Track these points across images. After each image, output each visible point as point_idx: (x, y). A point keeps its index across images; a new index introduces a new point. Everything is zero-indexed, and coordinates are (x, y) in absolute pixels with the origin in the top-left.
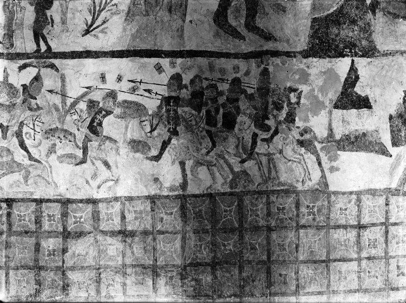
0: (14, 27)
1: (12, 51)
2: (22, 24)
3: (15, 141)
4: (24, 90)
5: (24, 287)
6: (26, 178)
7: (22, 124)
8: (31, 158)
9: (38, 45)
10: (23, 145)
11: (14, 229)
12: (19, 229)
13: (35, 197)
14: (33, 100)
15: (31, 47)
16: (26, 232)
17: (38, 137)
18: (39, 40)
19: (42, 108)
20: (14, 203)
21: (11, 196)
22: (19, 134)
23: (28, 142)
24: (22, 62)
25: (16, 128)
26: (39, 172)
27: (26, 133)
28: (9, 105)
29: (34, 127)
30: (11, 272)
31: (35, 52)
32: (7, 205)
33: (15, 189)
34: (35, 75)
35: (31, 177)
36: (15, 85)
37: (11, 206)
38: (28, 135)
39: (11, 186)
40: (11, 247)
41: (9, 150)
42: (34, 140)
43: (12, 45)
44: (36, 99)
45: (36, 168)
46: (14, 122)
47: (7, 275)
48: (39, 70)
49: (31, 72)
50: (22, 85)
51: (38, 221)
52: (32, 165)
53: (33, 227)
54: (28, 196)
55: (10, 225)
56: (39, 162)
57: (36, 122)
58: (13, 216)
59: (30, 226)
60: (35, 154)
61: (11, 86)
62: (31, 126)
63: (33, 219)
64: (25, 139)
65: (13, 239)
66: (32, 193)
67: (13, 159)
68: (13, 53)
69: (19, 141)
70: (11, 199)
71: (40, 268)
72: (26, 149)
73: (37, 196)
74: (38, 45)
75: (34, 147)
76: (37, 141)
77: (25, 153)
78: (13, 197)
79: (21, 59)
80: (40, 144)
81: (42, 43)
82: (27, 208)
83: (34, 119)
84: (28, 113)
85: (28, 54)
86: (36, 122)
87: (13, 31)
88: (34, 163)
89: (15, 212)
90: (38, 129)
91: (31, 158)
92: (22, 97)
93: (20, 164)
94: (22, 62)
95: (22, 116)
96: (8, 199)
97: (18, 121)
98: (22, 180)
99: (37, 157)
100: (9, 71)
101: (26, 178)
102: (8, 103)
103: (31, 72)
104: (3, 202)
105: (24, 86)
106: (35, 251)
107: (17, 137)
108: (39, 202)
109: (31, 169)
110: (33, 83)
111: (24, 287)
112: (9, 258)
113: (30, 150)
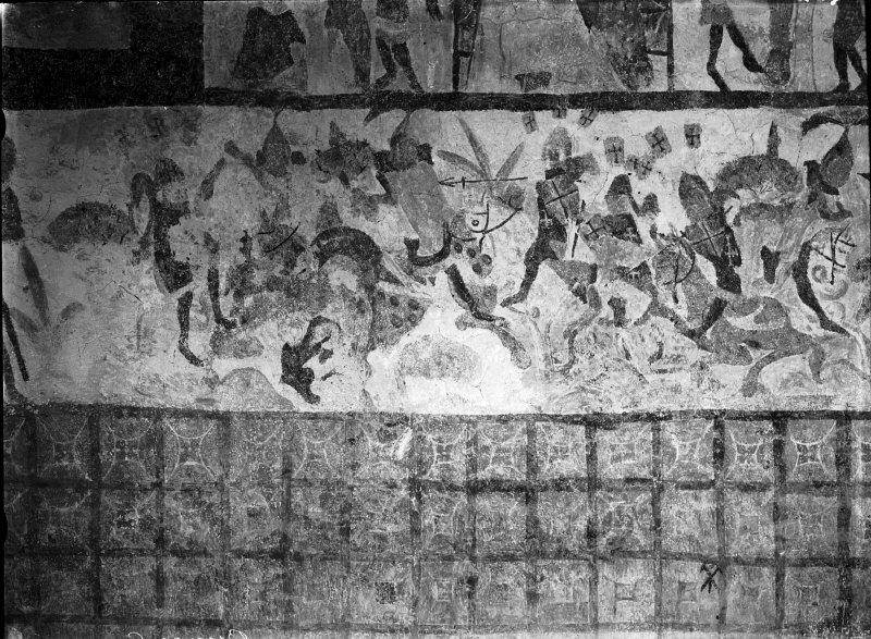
0: (792, 37)
1: (786, 88)
2: (810, 30)
3: (791, 285)
4: (809, 173)
5: (815, 604)
6: (817, 367)
7: (806, 249)
8: (825, 323)
9: (843, 75)
10: (807, 295)
11: (791, 477)
12: (801, 478)
13: (835, 408)
14: (830, 196)
15: (827, 79)
16: (818, 485)
17: (841, 276)
18: (845, 65)
19: (850, 214)
20: (790, 422)
21: (783, 406)
22: (799, 271)
23: (818, 288)
24: (809, 113)
25: (793, 258)
26: (844, 354)
27: (816, 269)
28: (780, 207)
29: (834, 254)
30: (789, 574)
31: (836, 91)
32: (774, 425)
33: (792, 392)
34: (835, 140)
35: (828, 365)
36: (793, 162)
37: (784, 426)
38: (818, 273)
39: (785, 384)
40: (786, 517)
41: (779, 305)
42: (832, 283)
43: (786, 76)
44: (837, 193)
45: (836, 345)
46: (791, 243)
47: (779, 577)
48: (847, 130)
49: (831, 134)
50: (806, 163)
51: (843, 461)
52: (827, 338)
53: (831, 473)
54: (820, 406)
55: (782, 469)
56: (842, 331)
57: (839, 245)
58: (787, 449)
59: (826, 472)
60: (832, 313)
61: (784, 165)
62: (828, 253)
63: (832, 455)
64: (812, 281)
65: (791, 499)
66: (828, 400)
67: (788, 324)
68: (789, 94)
69: (799, 287)
70: (783, 412)
71: (851, 563)
72: (812, 302)
73: (838, 406)
74: (843, 75)
75: (830, 297)
76: (836, 287)
77: (813, 313)
78: (787, 409)
79: (807, 107)
80: (842, 293)
81: (851, 71)
82: (819, 433)
83: (835, 236)
84: (822, 224)
85: (821, 94)
86: (839, 245)
87: (791, 46)
88: (832, 333)
89: (793, 441)
90: (841, 259)
91: (825, 323)
92: (806, 190)
93: (803, 335)
94: (809, 113)
95: (808, 231)
96: (776, 412)
97: (799, 241)
98: (809, 371)
99: (836, 320)
100: (780, 131)
101: (817, 367)
102: (776, 203)
103: (831, 134)
104: (767, 418)
105: (811, 165)
106: (839, 526)
107: (795, 277)
108: (845, 418)
109: (826, 347)
110: (831, 159)
111: (815, 604)
112: (784, 540)
113: (823, 304)
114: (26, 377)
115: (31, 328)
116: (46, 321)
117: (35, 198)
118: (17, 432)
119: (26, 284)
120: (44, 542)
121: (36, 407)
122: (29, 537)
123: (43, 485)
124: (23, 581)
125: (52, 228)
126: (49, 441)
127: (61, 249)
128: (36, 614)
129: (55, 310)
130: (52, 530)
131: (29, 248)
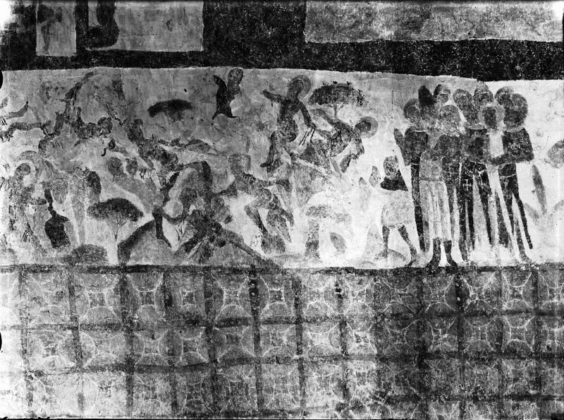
114: (531, 247)
115: (536, 216)
116: (544, 211)
117: (538, 135)
118: (526, 281)
119: (534, 188)
120: (544, 350)
121: (537, 266)
122: (535, 347)
123: (541, 314)
124: (531, 374)
125: (551, 154)
126: (545, 287)
127: (556, 166)
128: (538, 395)
129: (550, 206)
130: (549, 342)
131: (538, 166)
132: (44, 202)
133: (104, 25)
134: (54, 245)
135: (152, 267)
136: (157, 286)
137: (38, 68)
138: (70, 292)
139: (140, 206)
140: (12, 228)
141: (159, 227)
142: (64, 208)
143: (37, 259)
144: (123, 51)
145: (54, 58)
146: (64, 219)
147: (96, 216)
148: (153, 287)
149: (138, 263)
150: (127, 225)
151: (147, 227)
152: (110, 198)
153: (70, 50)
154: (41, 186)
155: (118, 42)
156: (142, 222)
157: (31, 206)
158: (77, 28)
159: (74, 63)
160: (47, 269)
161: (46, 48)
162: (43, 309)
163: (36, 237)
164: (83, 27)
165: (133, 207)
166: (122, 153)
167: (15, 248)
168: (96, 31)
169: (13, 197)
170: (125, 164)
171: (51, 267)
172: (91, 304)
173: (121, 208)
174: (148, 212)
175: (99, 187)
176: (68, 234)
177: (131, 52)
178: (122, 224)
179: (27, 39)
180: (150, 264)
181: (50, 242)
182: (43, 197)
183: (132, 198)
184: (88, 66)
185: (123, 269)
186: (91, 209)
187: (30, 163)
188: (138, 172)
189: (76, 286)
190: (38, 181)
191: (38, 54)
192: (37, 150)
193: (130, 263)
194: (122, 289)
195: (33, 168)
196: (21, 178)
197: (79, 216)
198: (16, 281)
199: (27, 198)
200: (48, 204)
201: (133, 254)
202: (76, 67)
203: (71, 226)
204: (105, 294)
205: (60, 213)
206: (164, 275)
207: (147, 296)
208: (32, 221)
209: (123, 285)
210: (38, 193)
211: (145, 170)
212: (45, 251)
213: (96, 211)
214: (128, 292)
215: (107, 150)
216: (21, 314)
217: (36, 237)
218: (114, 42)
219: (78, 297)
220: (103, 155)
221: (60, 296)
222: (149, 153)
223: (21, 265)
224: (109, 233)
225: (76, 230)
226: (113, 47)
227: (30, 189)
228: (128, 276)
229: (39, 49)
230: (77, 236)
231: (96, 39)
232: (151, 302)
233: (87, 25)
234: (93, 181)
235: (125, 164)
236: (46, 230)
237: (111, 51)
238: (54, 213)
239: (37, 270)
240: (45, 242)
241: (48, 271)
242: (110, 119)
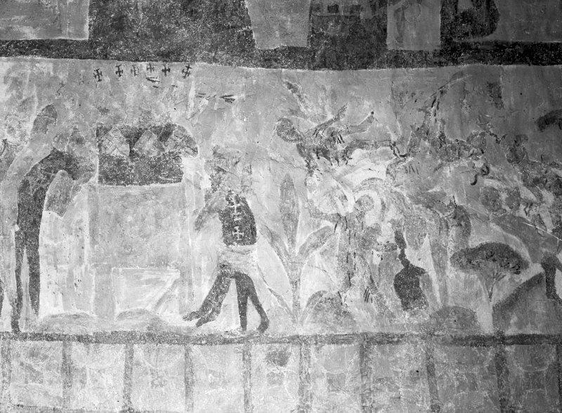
132: (394, 248)
133: (479, 6)
134: (406, 306)
135: (540, 337)
136: (548, 362)
137: (389, 66)
138: (429, 372)
139: (525, 253)
140: (349, 284)
141: (550, 283)
142: (420, 257)
143: (383, 326)
144: (503, 43)
145: (410, 53)
146: (420, 271)
147: (462, 267)
148: (542, 365)
149: (520, 332)
150: (507, 278)
151: (535, 281)
152: (484, 242)
153: (433, 42)
154: (390, 225)
155: (498, 31)
156: (524, 277)
157: (376, 253)
158: (442, 11)
159: (437, 60)
160: (396, 339)
161: (400, 39)
162: (394, 394)
163: (381, 296)
164: (450, 10)
165: (515, 255)
166: (499, 180)
167: (353, 309)
168: (466, 17)
169: (352, 240)
170: (504, 196)
171: (402, 336)
172: (458, 387)
173: (500, 256)
174: (534, 262)
175: (468, 226)
176: (425, 292)
177: (515, 44)
178: (498, 278)
179: (375, 27)
180: (538, 332)
181: (399, 303)
182: (393, 241)
183: (515, 243)
184: (455, 62)
185: (501, 340)
186: (456, 259)
187: (373, 194)
188: (522, 207)
189: (437, 362)
190: (386, 219)
191: (390, 48)
192: (384, 177)
193: (510, 332)
194: (499, 368)
195: (378, 203)
196: (362, 215)
197: (440, 267)
198: (356, 356)
199: (370, 243)
200: (399, 251)
201: (514, 319)
202: (440, 64)
203: (429, 281)
204: (476, 373)
205: (415, 263)
206: (557, 349)
207: (534, 377)
208: (377, 273)
209: (500, 364)
210: (386, 235)
211: (532, 205)
212: (392, 315)
213: (464, 260)
214: (507, 372)
215: (479, 178)
216: (363, 401)
217: (381, 296)
218: (492, 29)
219: (441, 377)
220: (474, 183)
221: (415, 376)
222: (536, 181)
223: (363, 334)
224: (480, 290)
225: (436, 286)
226: (490, 38)
227: (376, 230)
228: (507, 349)
229: (390, 43)
230: (438, 295)
231: (467, 27)
232: (539, 386)
233: (456, 9)
234: (461, 218)
235: (504, 196)
236: (395, 285)
237: (488, 43)
238: (406, 263)
239: (386, 340)
240: (392, 300)
241: (398, 342)
242: (483, 134)
